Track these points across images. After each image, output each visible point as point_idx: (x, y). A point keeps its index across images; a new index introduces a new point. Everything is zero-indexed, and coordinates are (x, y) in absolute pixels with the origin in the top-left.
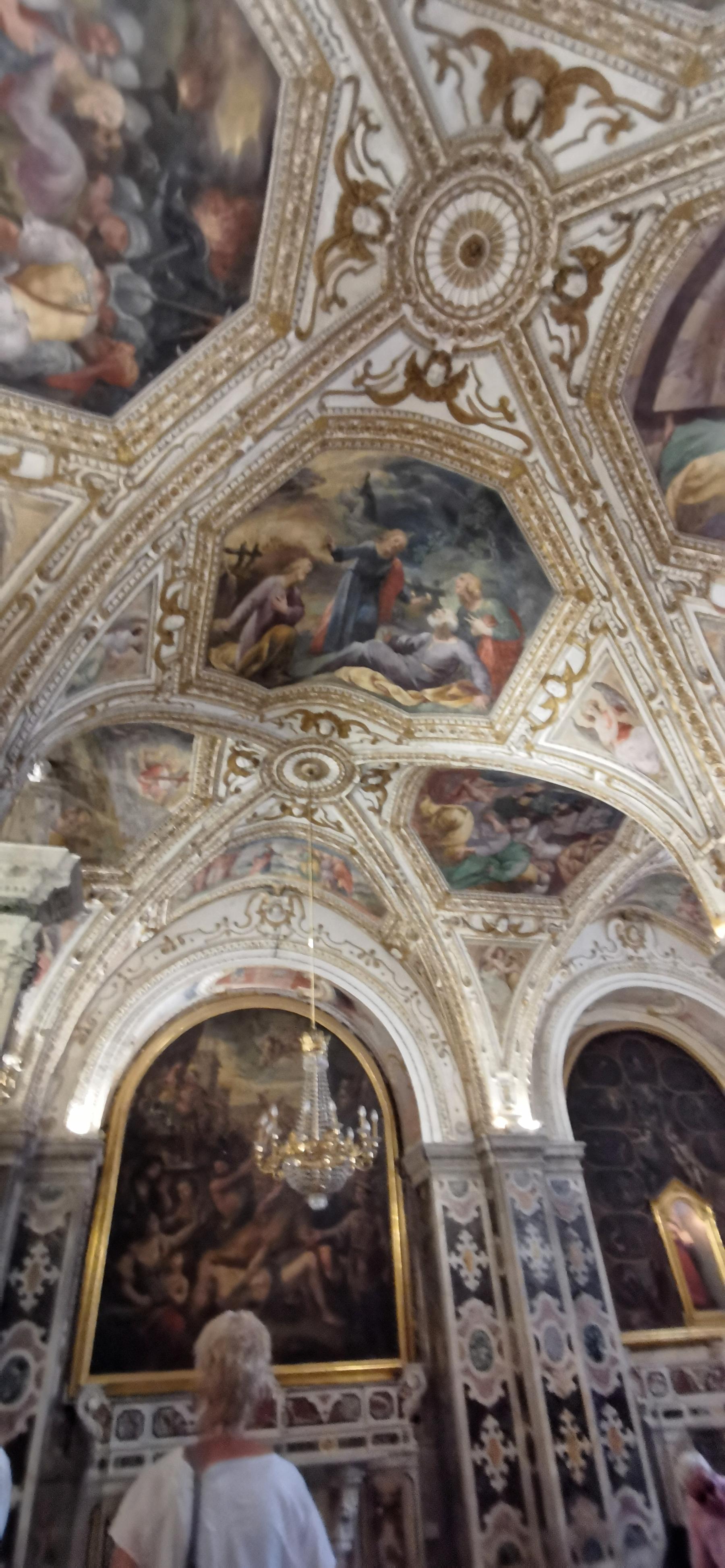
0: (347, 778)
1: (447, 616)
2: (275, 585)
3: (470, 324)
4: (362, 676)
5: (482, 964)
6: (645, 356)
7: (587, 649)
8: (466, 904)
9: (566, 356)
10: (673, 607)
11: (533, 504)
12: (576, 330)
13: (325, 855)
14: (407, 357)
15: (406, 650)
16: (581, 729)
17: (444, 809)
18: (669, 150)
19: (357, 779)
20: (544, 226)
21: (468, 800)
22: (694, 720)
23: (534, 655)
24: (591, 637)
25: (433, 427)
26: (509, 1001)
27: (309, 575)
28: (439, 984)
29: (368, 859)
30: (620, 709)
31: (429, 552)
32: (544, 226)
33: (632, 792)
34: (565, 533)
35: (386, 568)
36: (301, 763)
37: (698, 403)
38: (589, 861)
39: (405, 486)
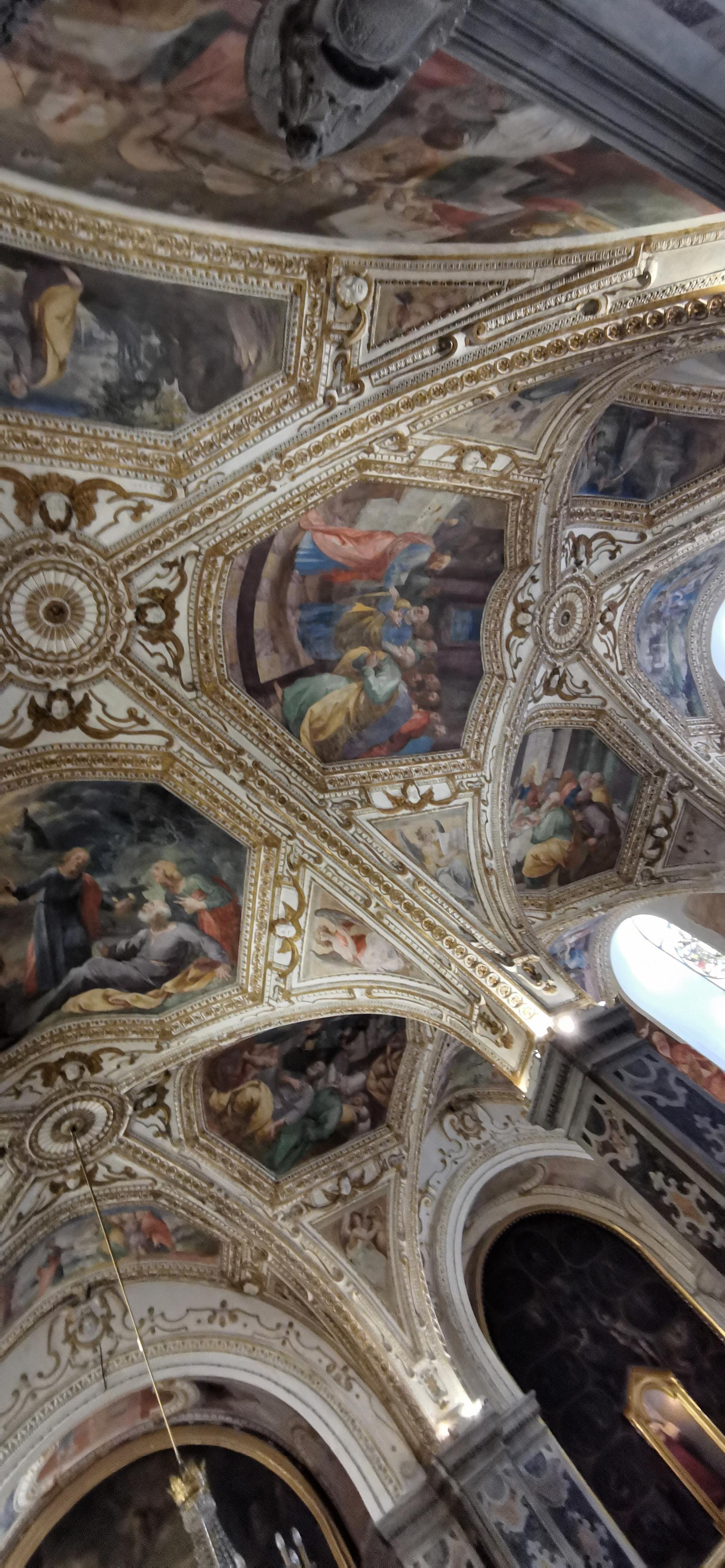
0: (118, 1114)
1: (157, 906)
3: (76, 663)
4: (93, 999)
5: (344, 1243)
6: (235, 647)
7: (296, 885)
8: (300, 1185)
9: (171, 664)
10: (348, 824)
11: (194, 783)
12: (170, 644)
13: (126, 1216)
14: (27, 702)
15: (130, 954)
16: (323, 957)
17: (236, 1094)
18: (185, 517)
19: (130, 1109)
20: (110, 583)
21: (254, 1072)
22: (409, 908)
23: (253, 909)
24: (294, 874)
25: (74, 751)
26: (388, 1269)
28: (310, 1297)
29: (176, 1193)
30: (348, 925)
31: (115, 856)
32: (110, 583)
33: (393, 994)
34: (232, 797)
35: (77, 887)
36: (57, 1125)
37: (292, 668)
38: (395, 1072)
39: (67, 809)
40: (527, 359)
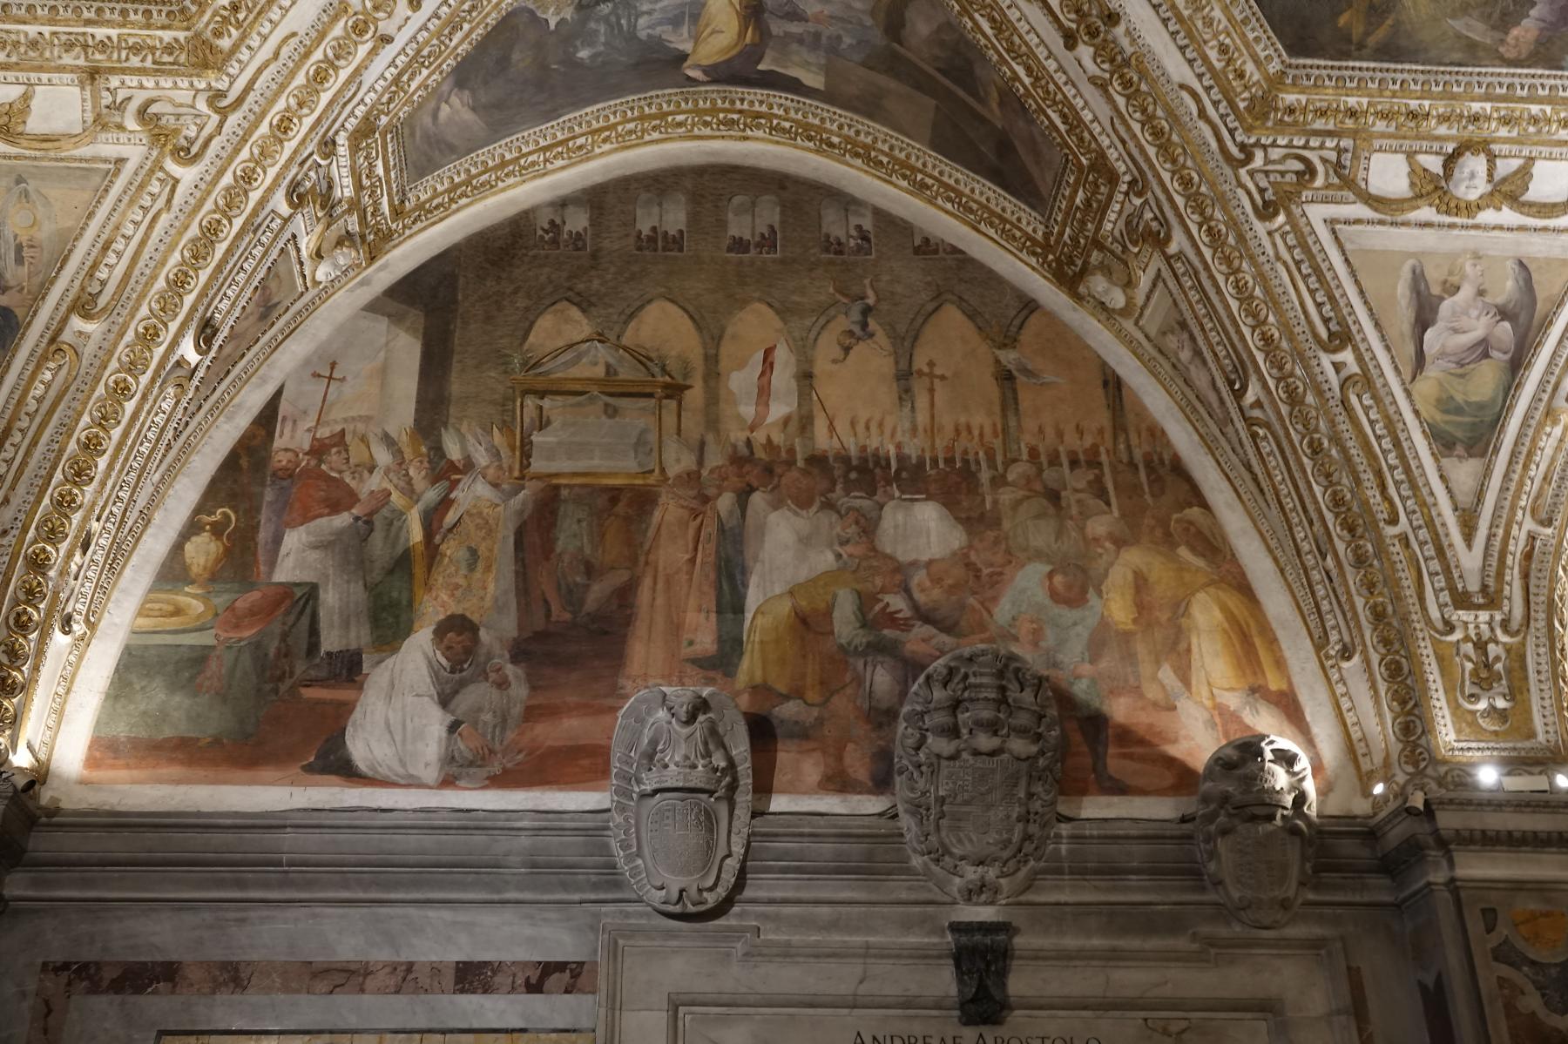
40: (103, 422)
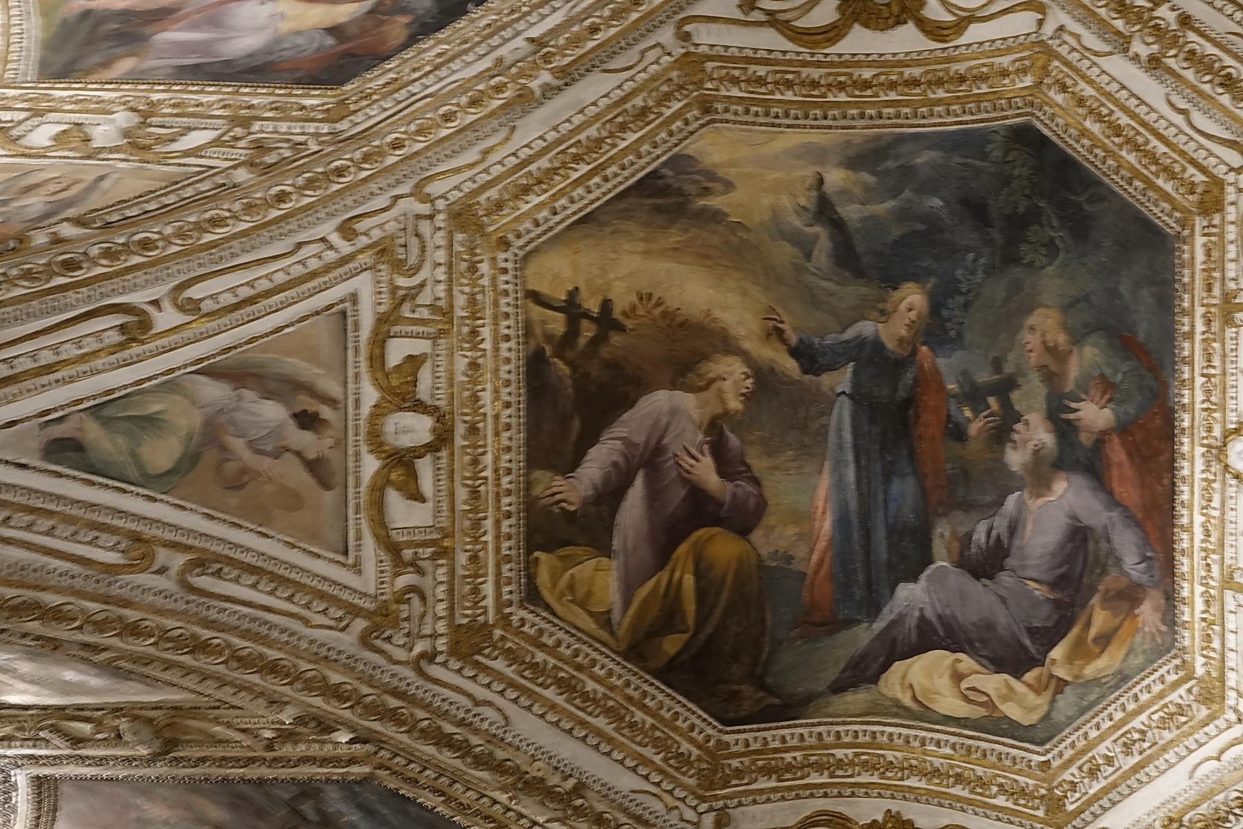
2: (674, 412)
27: (748, 398)
